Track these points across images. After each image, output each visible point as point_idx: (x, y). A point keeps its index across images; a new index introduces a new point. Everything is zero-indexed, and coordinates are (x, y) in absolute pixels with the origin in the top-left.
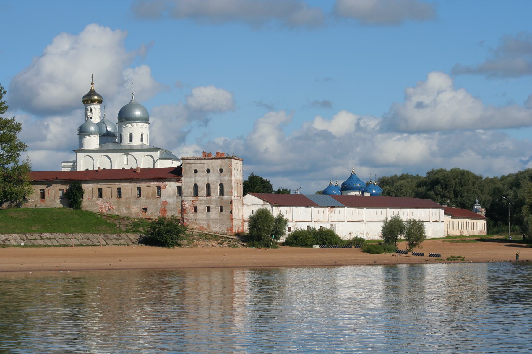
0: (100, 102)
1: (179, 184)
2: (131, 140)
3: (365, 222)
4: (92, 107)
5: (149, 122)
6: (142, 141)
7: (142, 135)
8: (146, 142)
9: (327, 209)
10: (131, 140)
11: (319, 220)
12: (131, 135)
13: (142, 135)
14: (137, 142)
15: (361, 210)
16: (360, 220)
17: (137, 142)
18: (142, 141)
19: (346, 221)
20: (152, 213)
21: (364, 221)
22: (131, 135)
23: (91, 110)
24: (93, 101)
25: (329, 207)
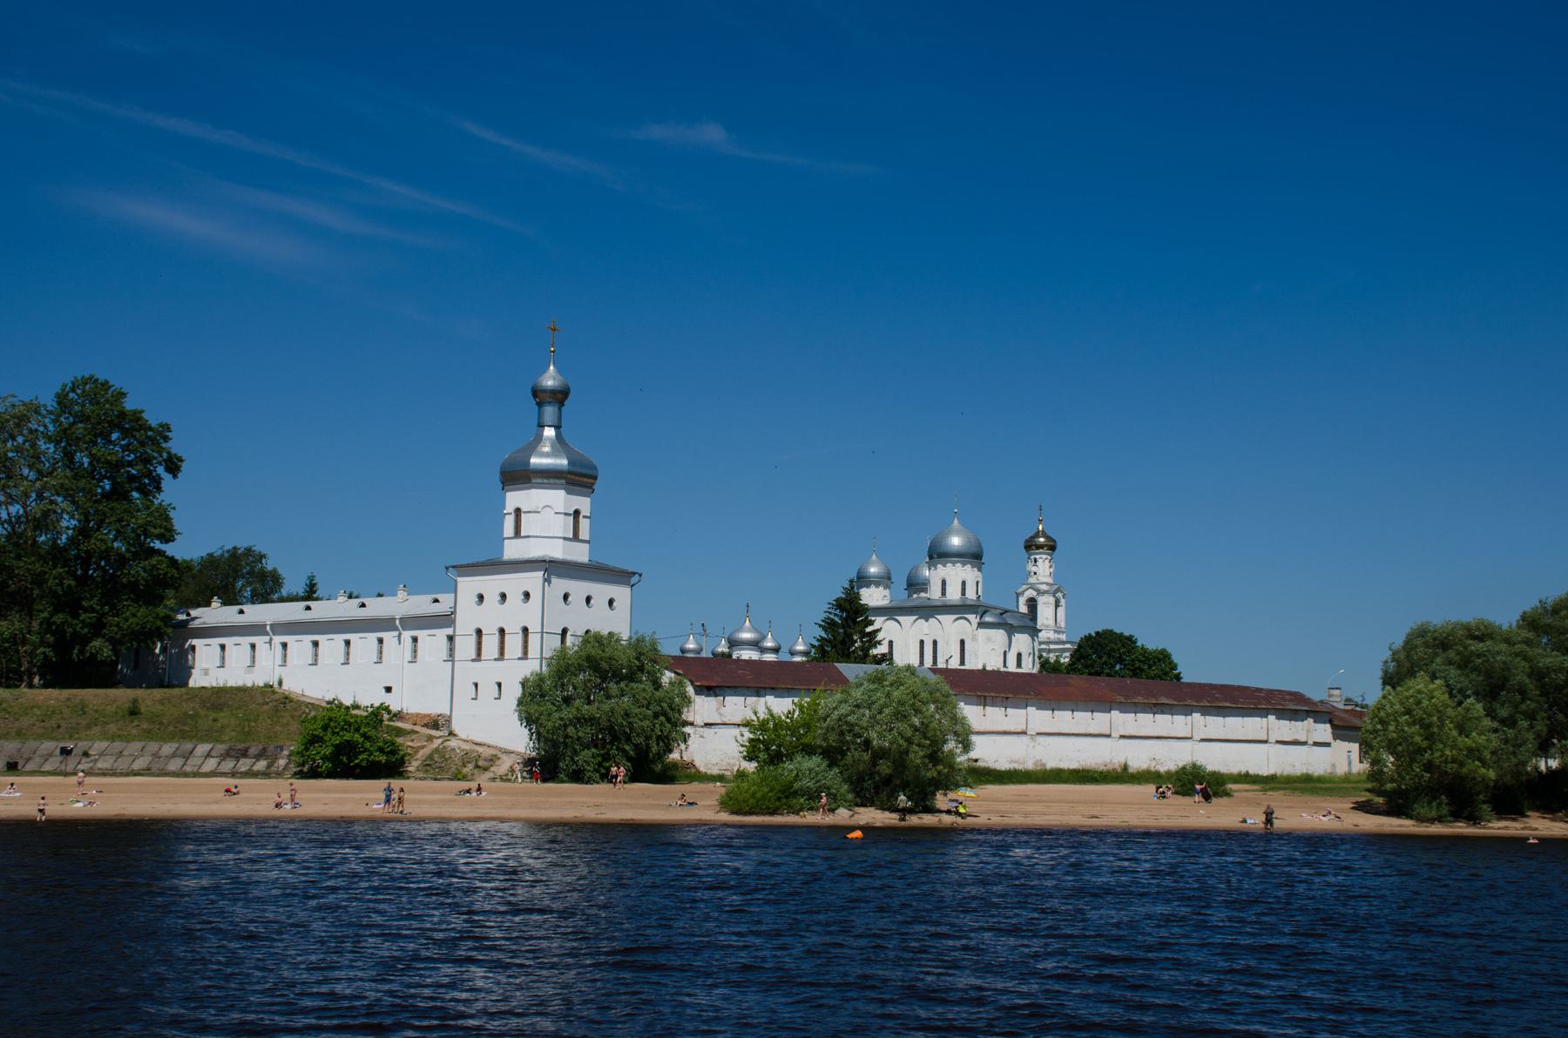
1: (449, 631)
2: (944, 593)
3: (1032, 735)
5: (983, 561)
6: (963, 593)
7: (964, 583)
8: (971, 594)
10: (944, 593)
12: (944, 583)
13: (964, 583)
14: (954, 595)
17: (934, 593)
18: (963, 593)
21: (1024, 733)
22: (944, 583)
23: (1036, 561)
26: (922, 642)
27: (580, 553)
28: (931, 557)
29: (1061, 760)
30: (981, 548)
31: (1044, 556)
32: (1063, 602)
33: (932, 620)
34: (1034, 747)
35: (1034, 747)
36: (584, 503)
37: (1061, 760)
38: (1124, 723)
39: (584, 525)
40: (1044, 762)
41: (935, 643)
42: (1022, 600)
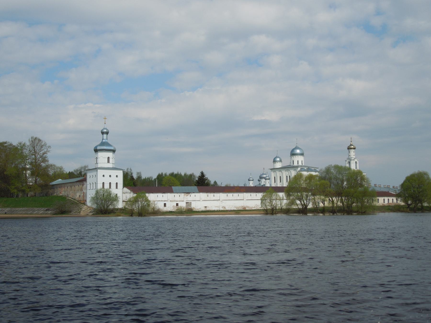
0: (354, 148)
4: (350, 151)
6: (298, 163)
7: (298, 161)
8: (300, 164)
9: (183, 194)
11: (174, 200)
13: (298, 161)
14: (296, 164)
15: (216, 194)
16: (216, 199)
18: (298, 163)
19: (201, 200)
20: (81, 198)
22: (293, 161)
23: (350, 152)
24: (351, 148)
25: (184, 193)
26: (287, 176)
27: (110, 165)
28: (291, 155)
29: (229, 206)
30: (304, 152)
31: (352, 151)
32: (358, 162)
33: (289, 172)
34: (222, 203)
35: (222, 203)
36: (110, 154)
37: (229, 206)
38: (248, 197)
39: (111, 160)
40: (225, 206)
41: (290, 176)
42: (347, 162)
